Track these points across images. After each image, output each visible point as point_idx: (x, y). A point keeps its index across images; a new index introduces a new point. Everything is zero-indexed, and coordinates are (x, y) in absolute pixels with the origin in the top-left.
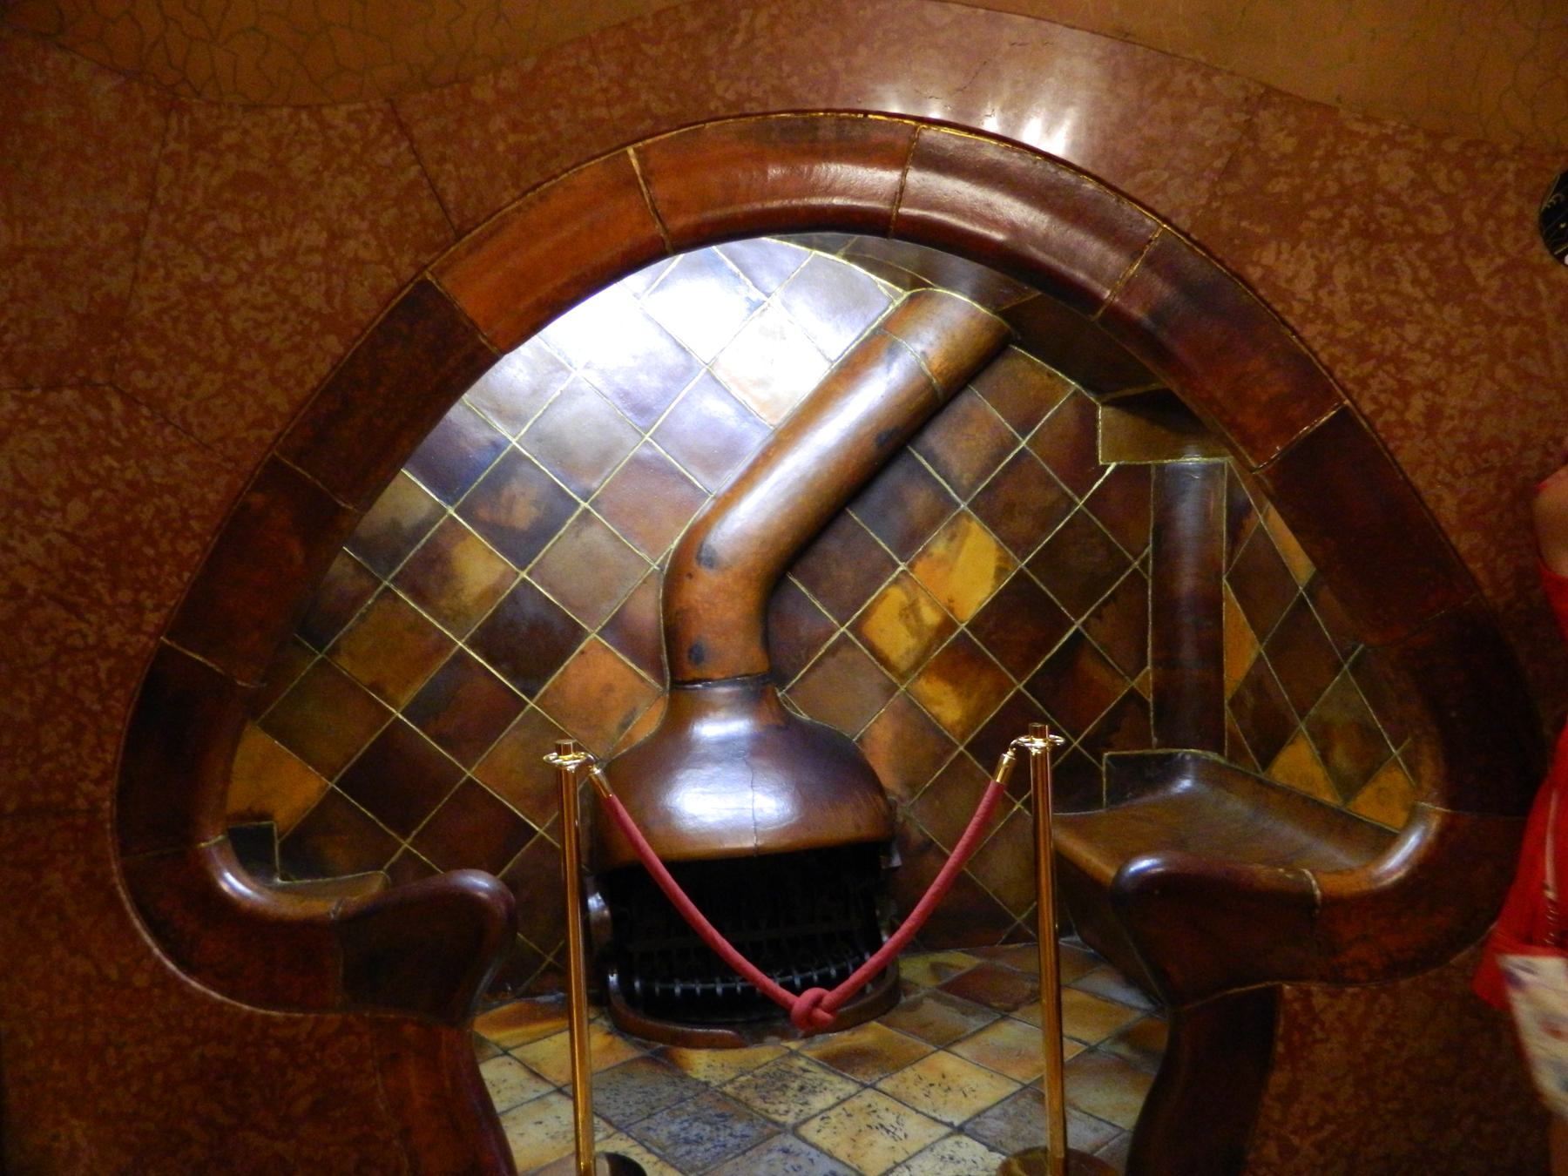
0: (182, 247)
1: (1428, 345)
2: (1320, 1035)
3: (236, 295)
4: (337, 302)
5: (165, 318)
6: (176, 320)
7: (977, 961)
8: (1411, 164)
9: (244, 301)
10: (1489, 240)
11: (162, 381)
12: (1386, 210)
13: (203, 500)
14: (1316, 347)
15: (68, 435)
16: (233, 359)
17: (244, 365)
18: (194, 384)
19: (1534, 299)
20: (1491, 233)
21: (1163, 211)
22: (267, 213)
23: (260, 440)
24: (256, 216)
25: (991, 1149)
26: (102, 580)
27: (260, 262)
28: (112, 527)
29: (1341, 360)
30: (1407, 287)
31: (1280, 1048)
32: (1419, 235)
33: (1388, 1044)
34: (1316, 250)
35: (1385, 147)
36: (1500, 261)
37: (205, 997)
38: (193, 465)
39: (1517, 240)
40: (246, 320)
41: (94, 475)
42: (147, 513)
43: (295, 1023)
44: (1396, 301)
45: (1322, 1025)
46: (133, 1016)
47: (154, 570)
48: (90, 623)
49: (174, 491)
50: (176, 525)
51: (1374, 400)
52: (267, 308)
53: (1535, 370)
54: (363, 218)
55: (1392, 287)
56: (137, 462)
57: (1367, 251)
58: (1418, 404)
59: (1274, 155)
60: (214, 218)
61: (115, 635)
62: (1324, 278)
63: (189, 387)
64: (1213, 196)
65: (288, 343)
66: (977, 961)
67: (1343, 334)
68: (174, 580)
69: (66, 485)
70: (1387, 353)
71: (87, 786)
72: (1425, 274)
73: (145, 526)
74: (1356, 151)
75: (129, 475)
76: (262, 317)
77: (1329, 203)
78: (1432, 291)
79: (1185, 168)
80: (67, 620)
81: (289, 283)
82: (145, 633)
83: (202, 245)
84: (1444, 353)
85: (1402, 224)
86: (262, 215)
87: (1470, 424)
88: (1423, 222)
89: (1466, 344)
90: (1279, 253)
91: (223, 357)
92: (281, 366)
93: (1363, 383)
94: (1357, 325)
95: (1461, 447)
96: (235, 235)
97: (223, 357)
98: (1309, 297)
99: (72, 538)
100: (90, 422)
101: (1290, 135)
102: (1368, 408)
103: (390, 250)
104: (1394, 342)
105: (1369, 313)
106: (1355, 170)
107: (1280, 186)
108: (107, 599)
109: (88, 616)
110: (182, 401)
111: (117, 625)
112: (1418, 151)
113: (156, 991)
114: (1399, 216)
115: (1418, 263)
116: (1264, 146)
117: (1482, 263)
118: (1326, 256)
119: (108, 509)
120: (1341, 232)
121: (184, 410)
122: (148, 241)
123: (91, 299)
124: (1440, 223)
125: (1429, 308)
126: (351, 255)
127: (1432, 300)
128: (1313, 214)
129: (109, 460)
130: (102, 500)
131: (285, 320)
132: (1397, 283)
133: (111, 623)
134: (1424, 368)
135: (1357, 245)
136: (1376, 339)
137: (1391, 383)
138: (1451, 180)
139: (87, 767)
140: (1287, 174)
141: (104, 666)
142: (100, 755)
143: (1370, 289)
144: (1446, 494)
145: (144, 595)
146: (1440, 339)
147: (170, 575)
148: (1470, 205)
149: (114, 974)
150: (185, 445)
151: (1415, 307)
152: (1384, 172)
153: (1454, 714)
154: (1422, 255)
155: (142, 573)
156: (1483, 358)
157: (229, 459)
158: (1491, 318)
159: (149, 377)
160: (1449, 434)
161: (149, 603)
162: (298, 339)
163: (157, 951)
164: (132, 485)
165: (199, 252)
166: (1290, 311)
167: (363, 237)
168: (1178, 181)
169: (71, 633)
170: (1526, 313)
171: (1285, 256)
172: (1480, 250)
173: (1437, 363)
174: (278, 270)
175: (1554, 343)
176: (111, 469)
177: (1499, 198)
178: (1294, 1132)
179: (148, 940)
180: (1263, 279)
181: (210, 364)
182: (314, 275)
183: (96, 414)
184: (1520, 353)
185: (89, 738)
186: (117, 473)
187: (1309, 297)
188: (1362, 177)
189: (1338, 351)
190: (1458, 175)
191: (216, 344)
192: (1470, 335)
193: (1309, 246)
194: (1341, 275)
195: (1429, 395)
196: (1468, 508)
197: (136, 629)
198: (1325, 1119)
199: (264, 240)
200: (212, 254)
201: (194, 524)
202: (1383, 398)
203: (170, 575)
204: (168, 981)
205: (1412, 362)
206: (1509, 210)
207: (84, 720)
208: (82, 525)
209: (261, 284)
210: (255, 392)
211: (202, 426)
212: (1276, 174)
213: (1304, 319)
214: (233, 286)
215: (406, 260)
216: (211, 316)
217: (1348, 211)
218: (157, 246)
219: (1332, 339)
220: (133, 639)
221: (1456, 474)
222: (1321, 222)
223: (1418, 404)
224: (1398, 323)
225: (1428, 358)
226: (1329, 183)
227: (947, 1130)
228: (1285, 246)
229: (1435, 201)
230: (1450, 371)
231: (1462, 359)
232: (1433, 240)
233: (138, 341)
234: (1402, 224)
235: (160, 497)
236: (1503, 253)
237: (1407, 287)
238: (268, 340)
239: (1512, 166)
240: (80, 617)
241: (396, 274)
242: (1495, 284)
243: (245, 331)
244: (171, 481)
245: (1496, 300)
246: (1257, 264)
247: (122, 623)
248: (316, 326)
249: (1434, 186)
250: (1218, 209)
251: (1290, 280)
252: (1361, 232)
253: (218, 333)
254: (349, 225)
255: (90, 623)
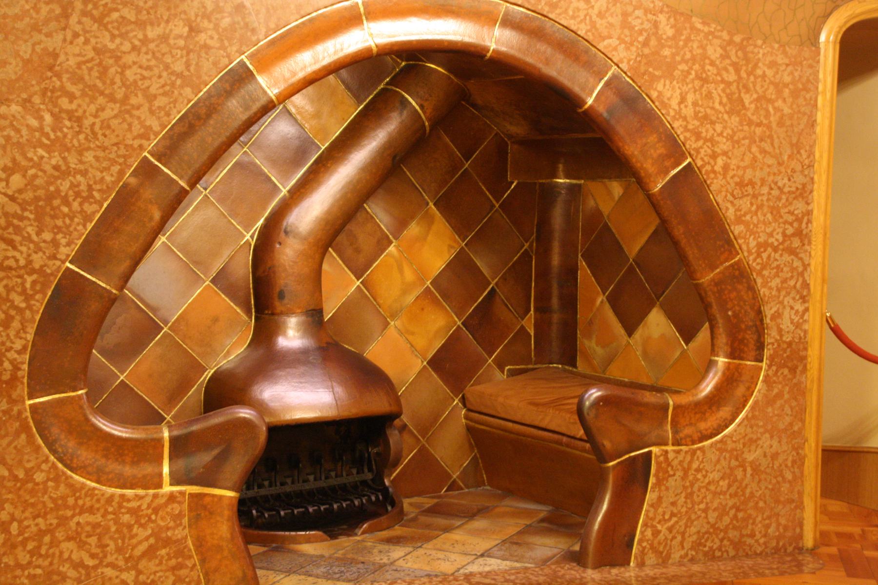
0: (96, 25)
1: (725, 134)
2: (671, 473)
3: (129, 59)
4: (192, 68)
5: (84, 67)
6: (90, 70)
7: (436, 501)
8: (720, 46)
9: (134, 63)
10: (751, 85)
11: (79, 106)
12: (710, 68)
13: (103, 178)
14: (679, 133)
15: (12, 133)
16: (126, 97)
17: (134, 101)
18: (103, 109)
19: (767, 115)
20: (753, 82)
21: (615, 61)
22: (152, 12)
23: (141, 147)
24: (145, 12)
25: (504, 560)
26: (31, 225)
27: (145, 41)
28: (41, 193)
29: (689, 139)
30: (717, 106)
31: (652, 480)
32: (723, 81)
33: (699, 476)
34: (680, 85)
35: (710, 37)
36: (755, 96)
37: (83, 485)
38: (97, 158)
39: (762, 86)
40: (136, 74)
41: (31, 160)
42: (65, 186)
43: (141, 498)
44: (713, 112)
45: (672, 467)
46: (32, 500)
47: (68, 221)
48: (22, 253)
49: (84, 173)
50: (85, 194)
51: (702, 159)
52: (149, 68)
53: (767, 148)
54: (210, 21)
55: (711, 105)
56: (60, 155)
57: (702, 86)
58: (720, 161)
59: (664, 37)
60: (116, 10)
61: (38, 260)
62: (683, 100)
63: (97, 111)
64: (638, 55)
65: (161, 91)
66: (436, 501)
67: (690, 127)
68: (80, 227)
69: (10, 165)
70: (708, 137)
71: (12, 355)
72: (725, 100)
73: (63, 194)
74: (699, 38)
75: (54, 162)
76: (146, 73)
77: (686, 62)
78: (727, 108)
79: (626, 39)
80: (6, 250)
81: (163, 55)
82: (60, 260)
83: (110, 26)
84: (730, 138)
85: (716, 75)
86: (148, 13)
87: (740, 173)
88: (725, 75)
89: (741, 135)
90: (665, 85)
91: (120, 95)
92: (157, 103)
93: (698, 151)
94: (697, 123)
95: (737, 184)
96: (132, 23)
97: (120, 95)
98: (677, 108)
99: (12, 199)
100: (28, 126)
101: (671, 27)
102: (699, 163)
103: (226, 43)
104: (711, 132)
105: (701, 117)
106: (698, 47)
107: (666, 52)
108: (35, 238)
109: (20, 248)
110: (91, 120)
111: (40, 254)
112: (724, 40)
113: (50, 484)
114: (715, 72)
115: (722, 94)
116: (660, 32)
117: (748, 96)
118: (685, 88)
119: (38, 182)
120: (691, 77)
121: (94, 124)
122: (74, 19)
123: (33, 50)
124: (732, 77)
125: (726, 116)
126: (202, 42)
127: (727, 113)
128: (680, 67)
129: (41, 152)
130: (35, 176)
131: (160, 77)
132: (713, 103)
133: (36, 253)
134: (724, 145)
135: (697, 83)
136: (704, 131)
137: (709, 151)
138: (737, 56)
139: (13, 343)
140: (670, 47)
141: (29, 279)
142: (23, 335)
143: (702, 106)
144: (729, 205)
145: (60, 236)
146: (730, 132)
147: (78, 224)
148: (744, 68)
149: (21, 475)
150: (92, 146)
151: (720, 116)
152: (710, 50)
153: (730, 313)
154: (723, 91)
155: (59, 223)
156: (747, 142)
157: (119, 156)
158: (750, 123)
159: (71, 102)
160: (732, 178)
161: (63, 241)
162: (167, 88)
163: (52, 458)
164: (56, 168)
165: (107, 30)
166: (668, 115)
167: (210, 33)
168: (623, 46)
169: (7, 258)
170: (765, 122)
171: (667, 87)
172: (748, 91)
173: (728, 143)
174: (157, 46)
175: (775, 136)
176: (42, 157)
177: (756, 66)
178: (659, 522)
179: (46, 450)
180: (658, 97)
181: (112, 99)
182: (179, 52)
183: (34, 123)
184: (761, 140)
185: (16, 324)
186: (45, 160)
187: (677, 108)
188: (700, 51)
189: (688, 135)
190: (740, 53)
191: (116, 87)
192: (742, 130)
193: (678, 83)
194: (690, 98)
195: (725, 158)
196: (739, 213)
197: (54, 257)
198: (673, 515)
199: (149, 28)
200: (116, 32)
201: (95, 194)
202: (706, 159)
203: (78, 224)
204: (57, 478)
205: (718, 142)
206: (759, 72)
207: (13, 312)
208: (20, 191)
209: (146, 53)
210: (139, 118)
211: (105, 136)
212: (663, 46)
213: (674, 118)
214: (129, 53)
215: (234, 49)
216: (112, 70)
217: (694, 67)
218: (79, 22)
219: (686, 129)
220: (51, 263)
221: (733, 196)
222: (682, 71)
223: (720, 161)
224: (713, 123)
225: (725, 140)
226: (687, 53)
227: (474, 557)
228: (668, 82)
229: (730, 65)
230: (734, 147)
231: (738, 142)
232: (729, 84)
233: (64, 80)
234: (716, 75)
235: (74, 177)
236: (757, 92)
237: (717, 106)
238: (148, 87)
239: (761, 51)
240: (15, 248)
241: (228, 56)
242: (753, 106)
243: (135, 82)
244: (82, 167)
245: (753, 114)
246: (656, 89)
247: (44, 253)
248: (179, 82)
249: (728, 57)
250: (640, 62)
251: (669, 99)
252: (698, 77)
253: (118, 79)
254: (201, 25)
255: (22, 253)
